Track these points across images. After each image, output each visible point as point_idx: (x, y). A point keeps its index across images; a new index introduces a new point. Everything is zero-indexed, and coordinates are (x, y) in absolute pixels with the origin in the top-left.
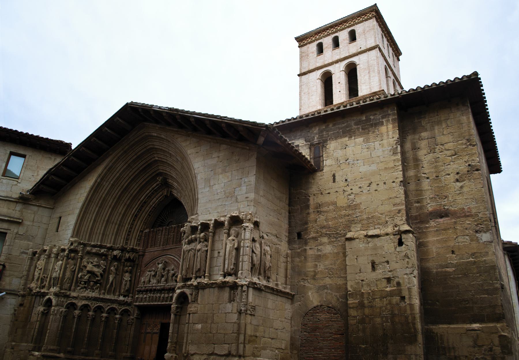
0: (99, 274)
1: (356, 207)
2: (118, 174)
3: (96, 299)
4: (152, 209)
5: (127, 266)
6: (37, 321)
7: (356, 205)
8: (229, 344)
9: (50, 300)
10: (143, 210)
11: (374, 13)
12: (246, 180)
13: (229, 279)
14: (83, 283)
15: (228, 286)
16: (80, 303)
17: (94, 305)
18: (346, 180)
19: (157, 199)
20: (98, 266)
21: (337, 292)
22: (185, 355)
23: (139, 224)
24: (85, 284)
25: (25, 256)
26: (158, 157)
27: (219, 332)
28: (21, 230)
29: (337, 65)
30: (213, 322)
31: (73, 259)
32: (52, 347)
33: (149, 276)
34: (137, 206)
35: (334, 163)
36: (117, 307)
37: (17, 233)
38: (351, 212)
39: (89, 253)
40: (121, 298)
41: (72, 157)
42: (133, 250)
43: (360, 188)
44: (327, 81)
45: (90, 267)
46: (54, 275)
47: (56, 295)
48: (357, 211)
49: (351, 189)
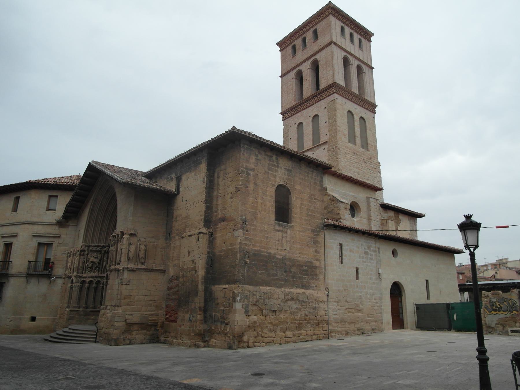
0: (97, 262)
3: (96, 277)
9: (72, 280)
11: (331, 10)
16: (88, 280)
17: (95, 280)
20: (97, 258)
25: (64, 255)
28: (60, 241)
29: (305, 64)
31: (83, 255)
39: (91, 251)
41: (75, 196)
44: (300, 77)
45: (92, 259)
47: (76, 277)
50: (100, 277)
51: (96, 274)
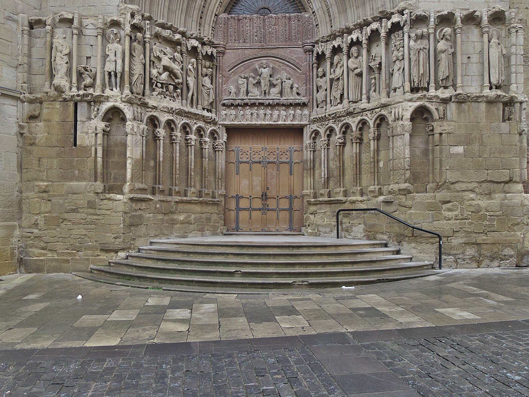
13: (499, 92)
16: (164, 118)
17: (180, 121)
20: (174, 59)
24: (162, 88)
32: (141, 186)
45: (166, 61)
50: (188, 115)
51: (176, 105)
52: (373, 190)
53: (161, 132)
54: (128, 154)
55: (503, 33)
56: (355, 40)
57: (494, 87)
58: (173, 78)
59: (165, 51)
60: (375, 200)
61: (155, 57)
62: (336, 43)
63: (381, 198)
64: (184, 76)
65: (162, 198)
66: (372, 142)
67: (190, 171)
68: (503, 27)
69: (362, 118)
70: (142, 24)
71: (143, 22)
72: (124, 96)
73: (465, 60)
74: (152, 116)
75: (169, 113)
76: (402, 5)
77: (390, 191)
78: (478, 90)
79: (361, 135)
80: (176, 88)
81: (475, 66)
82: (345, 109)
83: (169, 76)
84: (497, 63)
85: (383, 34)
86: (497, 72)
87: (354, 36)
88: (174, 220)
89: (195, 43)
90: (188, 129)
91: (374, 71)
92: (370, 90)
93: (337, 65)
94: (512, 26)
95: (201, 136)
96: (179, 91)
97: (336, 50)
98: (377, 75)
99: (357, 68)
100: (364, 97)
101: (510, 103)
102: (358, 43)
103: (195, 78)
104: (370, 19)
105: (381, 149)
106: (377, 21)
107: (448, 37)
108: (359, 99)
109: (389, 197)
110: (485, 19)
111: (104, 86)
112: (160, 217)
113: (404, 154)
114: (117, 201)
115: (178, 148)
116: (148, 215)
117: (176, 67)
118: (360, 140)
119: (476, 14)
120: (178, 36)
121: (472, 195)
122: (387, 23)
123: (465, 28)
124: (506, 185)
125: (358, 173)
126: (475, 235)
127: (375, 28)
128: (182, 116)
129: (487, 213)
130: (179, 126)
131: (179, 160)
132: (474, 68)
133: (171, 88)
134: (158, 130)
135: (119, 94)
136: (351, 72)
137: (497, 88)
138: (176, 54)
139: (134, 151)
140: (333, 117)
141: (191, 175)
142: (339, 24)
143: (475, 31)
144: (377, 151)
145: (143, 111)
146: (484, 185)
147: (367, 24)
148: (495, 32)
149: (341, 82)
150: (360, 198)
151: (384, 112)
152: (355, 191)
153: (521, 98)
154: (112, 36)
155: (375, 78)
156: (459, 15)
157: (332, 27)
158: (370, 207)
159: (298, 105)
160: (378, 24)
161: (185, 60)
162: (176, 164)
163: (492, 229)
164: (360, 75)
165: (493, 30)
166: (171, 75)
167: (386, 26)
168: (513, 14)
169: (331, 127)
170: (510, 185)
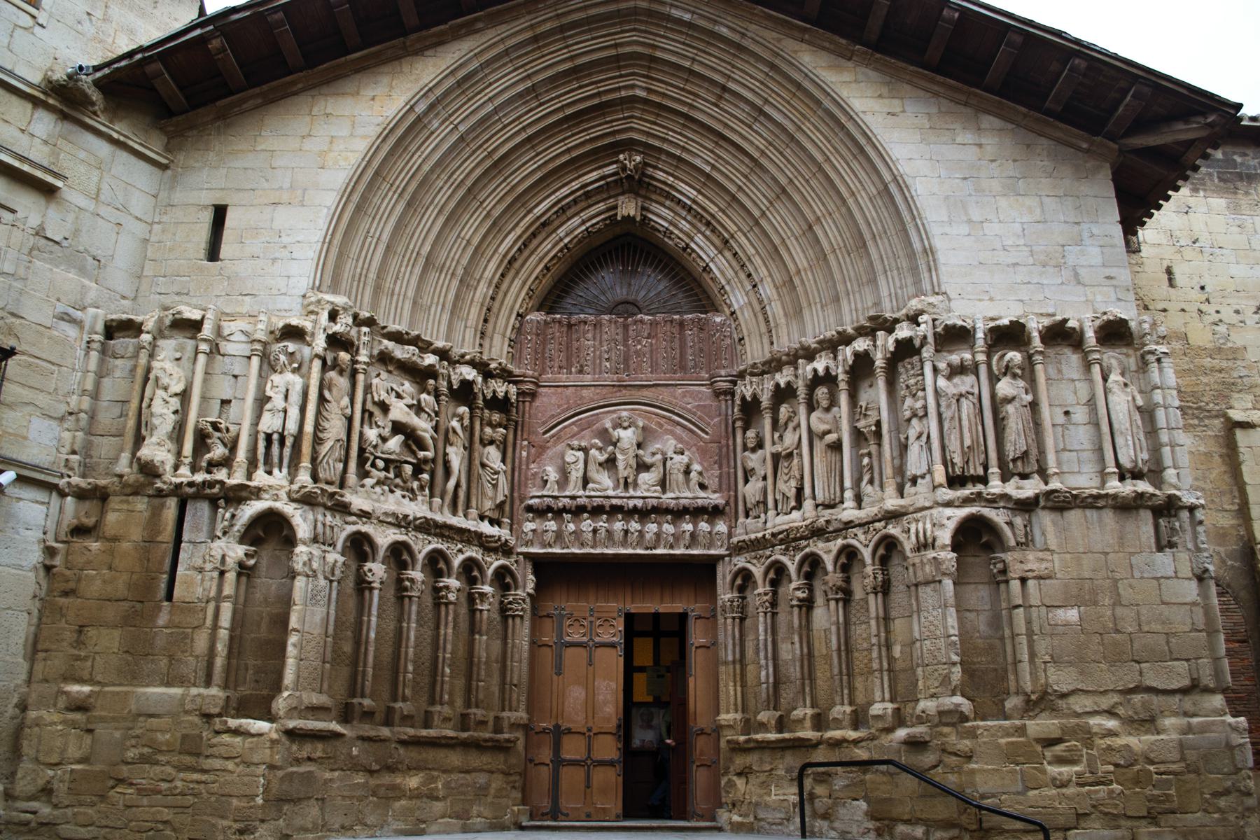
1: (1236, 354)
2: (490, 107)
3: (427, 527)
4: (561, 250)
5: (490, 424)
6: (219, 598)
7: (1234, 350)
8: (1187, 660)
10: (532, 246)
12: (1095, 231)
13: (1143, 486)
14: (381, 464)
15: (1147, 507)
16: (384, 537)
17: (423, 546)
18: (1202, 288)
19: (583, 222)
20: (418, 409)
21: (1220, 545)
22: (1033, 697)
23: (516, 294)
24: (386, 469)
25: (71, 331)
26: (649, 91)
27: (1146, 628)
28: (56, 221)
30: (1117, 602)
33: (581, 465)
34: (519, 231)
35: (1164, 242)
36: (480, 557)
37: (40, 232)
38: (1224, 364)
40: (486, 528)
42: (506, 375)
43: (1237, 312)
45: (399, 411)
46: (270, 423)
48: (1239, 363)
49: (1218, 312)
51: (417, 509)
52: (880, 712)
53: (377, 570)
54: (294, 622)
55: (1132, 362)
56: (821, 371)
57: (1128, 475)
58: (414, 448)
59: (400, 391)
60: (885, 740)
61: (374, 403)
62: (782, 378)
63: (902, 733)
64: (441, 445)
65: (368, 730)
66: (871, 597)
67: (440, 666)
68: (1131, 352)
69: (845, 542)
70: (354, 332)
71: (355, 330)
72: (295, 487)
73: (1061, 419)
74: (358, 533)
75: (398, 526)
76: (915, 304)
77: (919, 717)
78: (1096, 482)
79: (847, 580)
80: (417, 470)
81: (1082, 429)
82: (808, 522)
83: (405, 444)
84: (1128, 425)
85: (879, 362)
86: (1130, 443)
87: (820, 365)
88: (393, 787)
89: (469, 373)
90: (442, 565)
91: (866, 439)
92: (860, 479)
93: (786, 424)
94: (1146, 348)
95: (472, 581)
96: (426, 476)
97: (783, 394)
98: (873, 449)
99: (829, 432)
100: (848, 494)
101: (1168, 508)
102: (828, 379)
103: (465, 448)
104: (850, 330)
105: (893, 614)
106: (866, 335)
107: (1019, 372)
108: (837, 500)
109: (919, 730)
110: (1090, 335)
111: (252, 464)
112: (360, 779)
113: (945, 627)
114: (253, 735)
115: (414, 608)
116: (328, 775)
117: (423, 425)
118: (845, 596)
119: (1070, 324)
120: (430, 359)
121: (1112, 724)
122: (886, 341)
123: (1051, 352)
124: (1186, 698)
125: (845, 671)
126: (1129, 823)
127: (861, 349)
128: (429, 534)
129: (1151, 768)
130: (420, 557)
131: (416, 638)
132: (1081, 436)
133: (408, 469)
134: (369, 565)
135: (285, 483)
136: (817, 443)
137: (1137, 475)
138: (424, 396)
139: (310, 614)
140: (782, 540)
141: (443, 676)
142: (786, 341)
143: (1072, 359)
144: (886, 619)
145: (338, 521)
146: (1137, 698)
147: (846, 339)
148: (1114, 362)
149: (795, 461)
150: (852, 735)
151: (893, 530)
152: (840, 717)
153: (1188, 499)
154: (283, 358)
155: (869, 455)
156: (1035, 326)
157: (772, 343)
158: (876, 757)
159: (697, 512)
160: (868, 342)
161: (443, 409)
162: (407, 647)
163: (1167, 806)
164: (836, 447)
165: (1111, 357)
166: (410, 442)
167: (885, 346)
168: (1146, 326)
169: (777, 562)
170: (1196, 697)
